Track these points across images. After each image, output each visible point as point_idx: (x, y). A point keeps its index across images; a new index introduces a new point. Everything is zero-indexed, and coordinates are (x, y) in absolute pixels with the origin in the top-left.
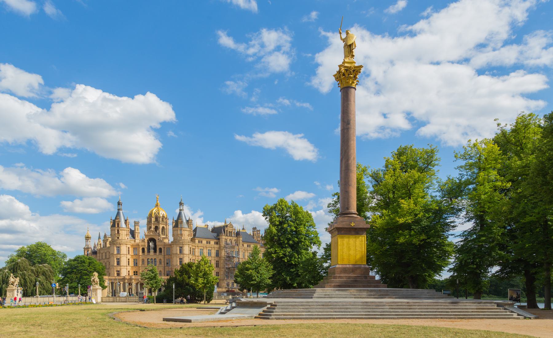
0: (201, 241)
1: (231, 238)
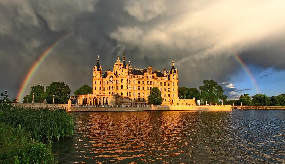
1: (150, 74)
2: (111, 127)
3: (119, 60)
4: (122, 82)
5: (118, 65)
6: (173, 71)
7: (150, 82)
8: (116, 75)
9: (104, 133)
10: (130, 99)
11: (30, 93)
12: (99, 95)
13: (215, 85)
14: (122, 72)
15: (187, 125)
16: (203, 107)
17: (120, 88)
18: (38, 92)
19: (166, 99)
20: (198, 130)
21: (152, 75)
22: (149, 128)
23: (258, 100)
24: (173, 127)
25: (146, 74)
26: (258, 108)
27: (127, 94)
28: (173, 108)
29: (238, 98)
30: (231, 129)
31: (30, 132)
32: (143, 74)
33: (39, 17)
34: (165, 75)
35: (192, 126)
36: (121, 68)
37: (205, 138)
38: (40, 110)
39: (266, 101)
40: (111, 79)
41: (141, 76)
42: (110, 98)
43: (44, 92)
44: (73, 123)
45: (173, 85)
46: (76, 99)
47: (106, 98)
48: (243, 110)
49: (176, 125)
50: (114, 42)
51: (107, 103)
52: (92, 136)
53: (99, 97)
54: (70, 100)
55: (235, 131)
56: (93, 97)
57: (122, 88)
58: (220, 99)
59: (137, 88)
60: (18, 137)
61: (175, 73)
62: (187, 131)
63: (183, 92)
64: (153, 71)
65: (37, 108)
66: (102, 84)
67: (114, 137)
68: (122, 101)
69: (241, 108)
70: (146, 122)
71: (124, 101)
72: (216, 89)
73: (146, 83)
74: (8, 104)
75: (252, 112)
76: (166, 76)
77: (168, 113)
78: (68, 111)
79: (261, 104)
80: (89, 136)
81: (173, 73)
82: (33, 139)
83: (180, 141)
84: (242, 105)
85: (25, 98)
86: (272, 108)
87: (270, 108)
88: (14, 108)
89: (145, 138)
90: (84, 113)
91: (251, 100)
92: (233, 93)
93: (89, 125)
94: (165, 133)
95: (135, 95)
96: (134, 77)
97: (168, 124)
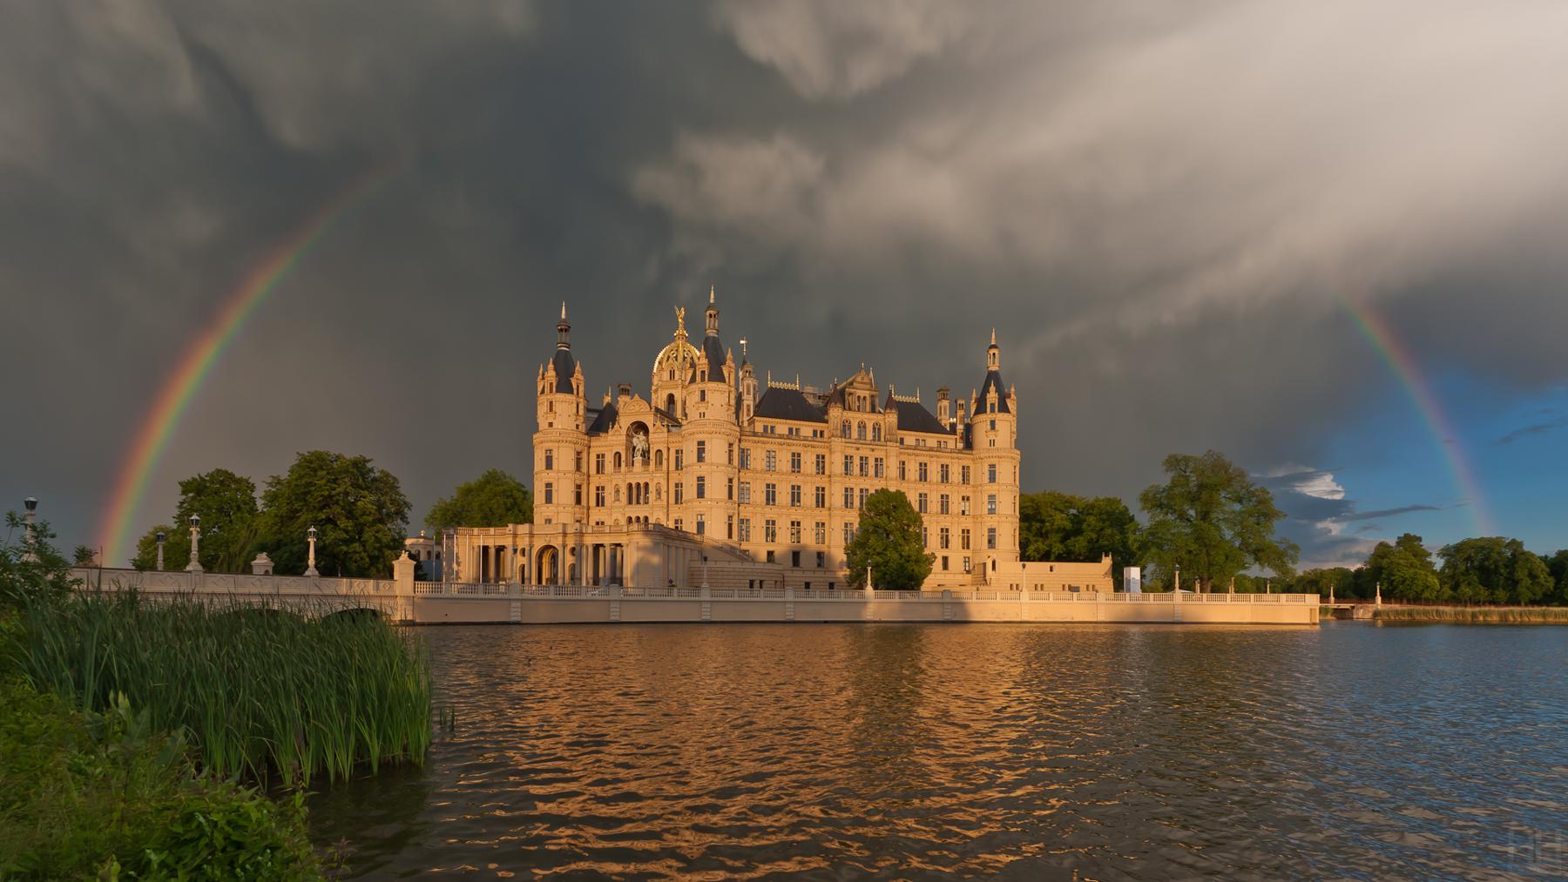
0: (772, 428)
1: (866, 416)
2: (639, 710)
3: (681, 331)
4: (700, 458)
5: (680, 359)
6: (992, 396)
7: (857, 461)
8: (669, 415)
9: (599, 742)
10: (745, 556)
11: (176, 512)
12: (570, 530)
13: (1230, 480)
14: (703, 398)
15: (1064, 706)
16: (1155, 604)
17: (690, 491)
18: (220, 510)
19: (945, 559)
20: (1122, 735)
21: (870, 419)
22: (848, 719)
23: (1475, 568)
24: (982, 713)
25: (835, 413)
26: (1474, 615)
27: (730, 526)
28: (989, 607)
29: (1358, 556)
30: (1306, 731)
31: (181, 731)
32: (819, 415)
33: (205, 60)
34: (946, 420)
35: (1090, 709)
36: (693, 380)
37: (1162, 776)
38: (235, 612)
39: (1521, 574)
40: (639, 441)
41: (807, 428)
42: (633, 547)
43: (253, 510)
44: (424, 684)
45: (992, 478)
46: (438, 556)
47: (608, 550)
48: (1388, 624)
49: (1000, 702)
50: (658, 221)
51: (616, 579)
52: (535, 755)
53: (571, 543)
54: (404, 556)
55: (1329, 744)
56: (539, 544)
57: (701, 494)
58: (1257, 559)
59: (783, 496)
60: (114, 762)
61: (1004, 408)
62: (1063, 737)
63: (1043, 522)
64: (877, 401)
65: (215, 600)
66: (584, 469)
67: (657, 762)
68: (698, 564)
69: (1376, 614)
70: (833, 682)
71: (710, 564)
72: (1237, 507)
73: (836, 464)
74: (50, 577)
75: (1437, 638)
76: (953, 426)
77: (955, 634)
78: (397, 617)
79: (1492, 594)
80: (518, 757)
81: (992, 411)
82: (199, 769)
83: (1019, 792)
84: (1379, 599)
85: (148, 544)
86: (1551, 619)
87: (1544, 615)
88: (85, 602)
89: (828, 769)
90: (487, 631)
91: (1434, 572)
92: (1335, 528)
93: (516, 700)
94: (937, 747)
95: (771, 534)
96: (769, 432)
97: (957, 697)
